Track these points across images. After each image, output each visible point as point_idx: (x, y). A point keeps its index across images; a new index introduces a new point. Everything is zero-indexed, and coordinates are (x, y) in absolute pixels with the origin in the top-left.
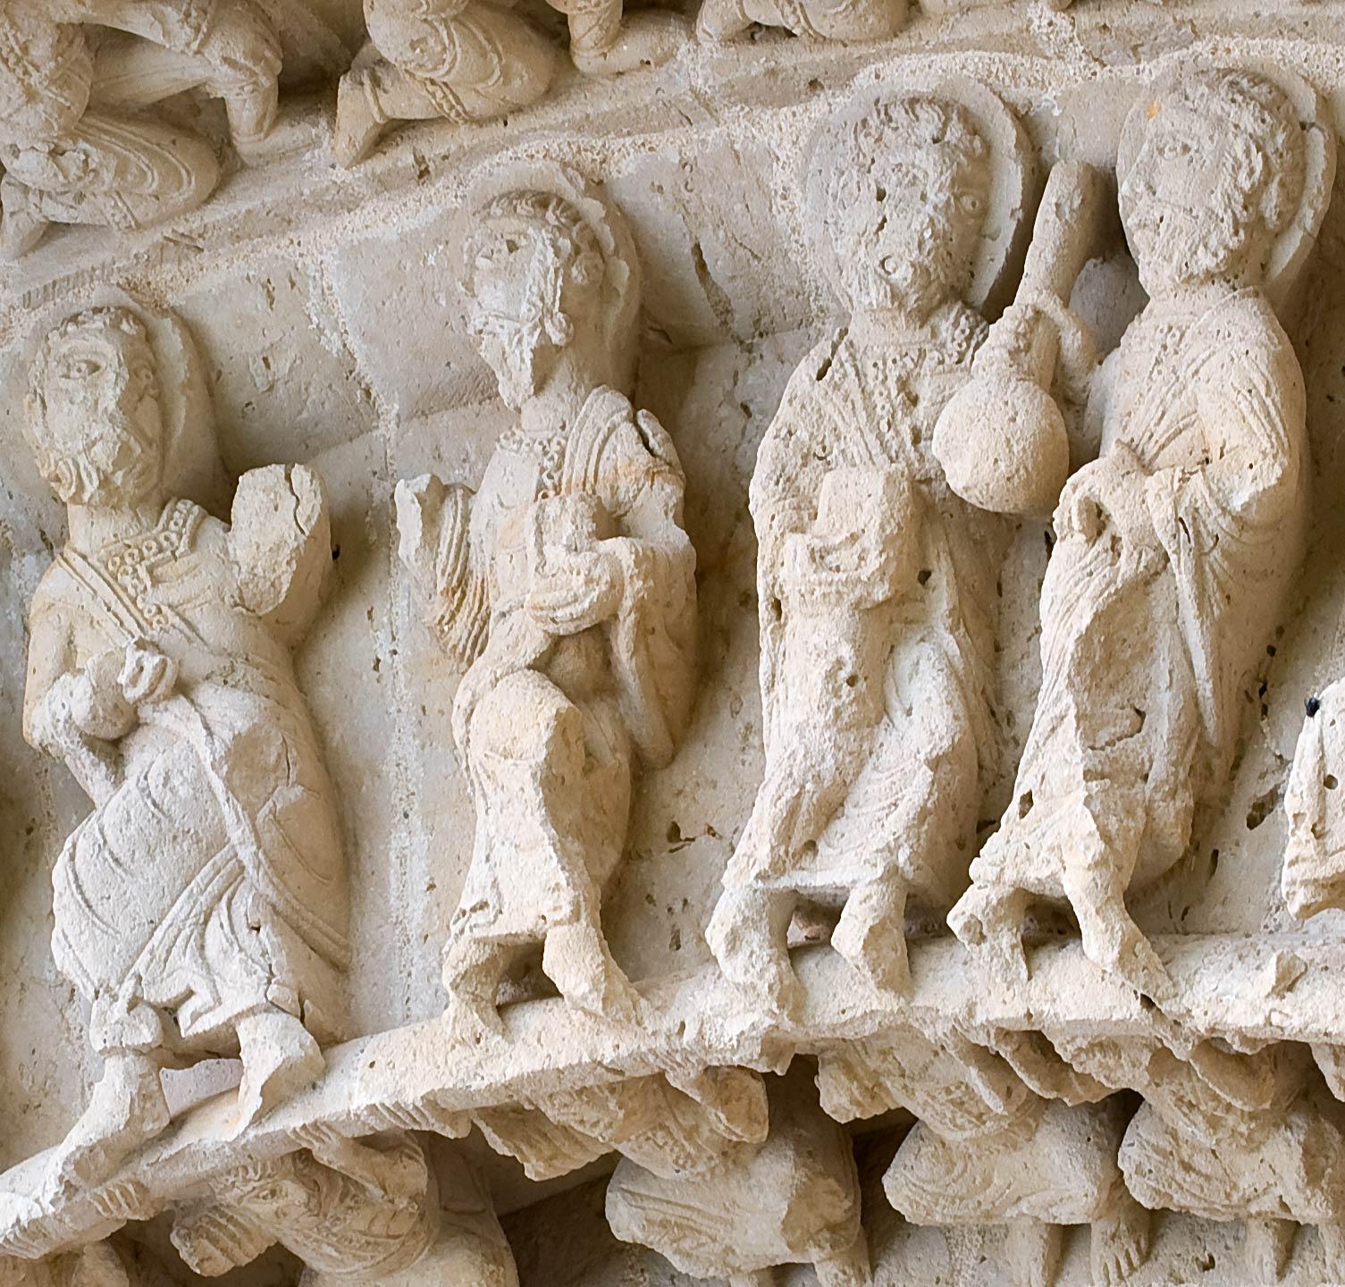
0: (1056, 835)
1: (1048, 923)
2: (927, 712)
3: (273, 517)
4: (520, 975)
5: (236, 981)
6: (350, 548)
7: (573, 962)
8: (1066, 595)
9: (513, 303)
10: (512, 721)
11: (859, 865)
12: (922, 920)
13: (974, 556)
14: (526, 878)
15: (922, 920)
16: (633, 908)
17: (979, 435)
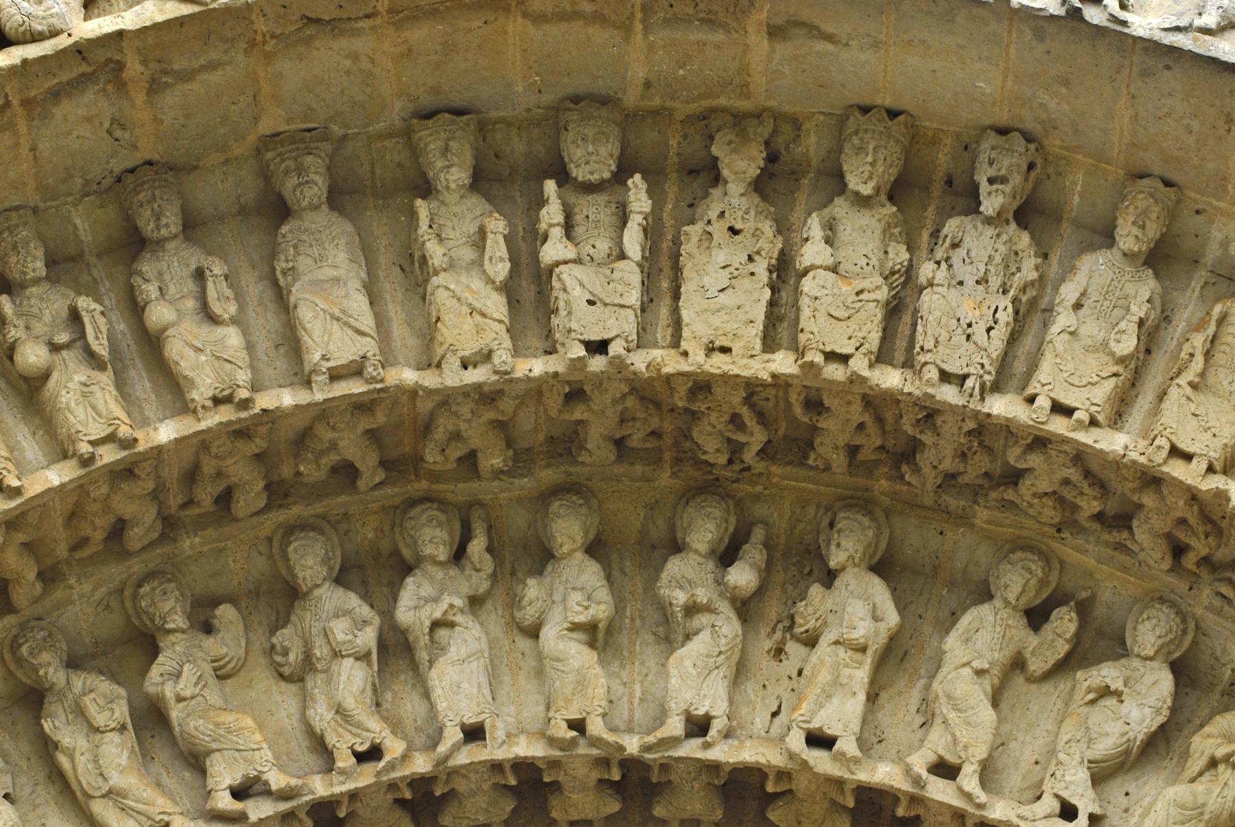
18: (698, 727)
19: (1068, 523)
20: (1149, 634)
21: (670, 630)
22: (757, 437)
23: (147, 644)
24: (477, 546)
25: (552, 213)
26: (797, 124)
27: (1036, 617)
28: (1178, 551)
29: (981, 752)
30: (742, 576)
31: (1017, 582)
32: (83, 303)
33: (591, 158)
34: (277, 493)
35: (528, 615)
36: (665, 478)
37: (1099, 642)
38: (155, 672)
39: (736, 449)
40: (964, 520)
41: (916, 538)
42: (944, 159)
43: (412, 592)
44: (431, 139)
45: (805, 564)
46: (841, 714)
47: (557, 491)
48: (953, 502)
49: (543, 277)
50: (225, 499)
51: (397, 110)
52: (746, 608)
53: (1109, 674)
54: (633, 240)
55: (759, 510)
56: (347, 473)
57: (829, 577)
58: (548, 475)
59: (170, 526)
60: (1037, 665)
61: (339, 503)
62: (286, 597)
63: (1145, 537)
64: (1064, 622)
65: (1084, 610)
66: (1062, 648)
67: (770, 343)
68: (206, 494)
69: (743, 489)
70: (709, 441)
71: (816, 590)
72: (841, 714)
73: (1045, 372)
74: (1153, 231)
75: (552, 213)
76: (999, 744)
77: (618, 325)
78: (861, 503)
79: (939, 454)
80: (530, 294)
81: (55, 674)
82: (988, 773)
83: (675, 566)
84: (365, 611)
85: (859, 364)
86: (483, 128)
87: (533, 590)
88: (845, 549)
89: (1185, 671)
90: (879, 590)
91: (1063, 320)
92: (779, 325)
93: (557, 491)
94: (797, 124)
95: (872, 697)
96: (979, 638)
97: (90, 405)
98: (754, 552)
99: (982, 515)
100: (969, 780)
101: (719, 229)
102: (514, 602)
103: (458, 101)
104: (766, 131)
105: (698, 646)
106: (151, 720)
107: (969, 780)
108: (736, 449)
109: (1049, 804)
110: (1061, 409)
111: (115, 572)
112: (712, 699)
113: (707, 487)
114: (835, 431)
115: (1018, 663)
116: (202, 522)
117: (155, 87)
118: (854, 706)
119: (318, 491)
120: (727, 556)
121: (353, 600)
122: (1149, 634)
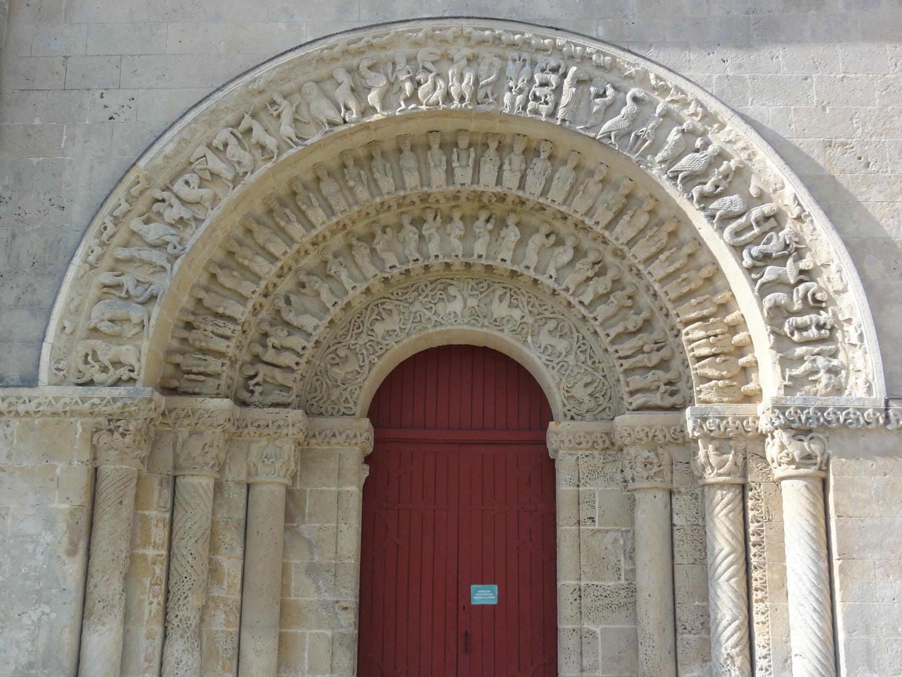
0: (627, 364)
1: (622, 365)
2: (629, 353)
3: (629, 303)
4: (608, 335)
5: (600, 319)
6: (630, 308)
7: (609, 339)
8: (639, 357)
9: (645, 315)
10: (619, 328)
11: (621, 354)
12: (620, 358)
13: (640, 351)
14: (613, 333)
15: (620, 358)
16: (613, 342)
17: (646, 348)
18: (480, 256)
19: (555, 218)
20: (570, 242)
21: (476, 237)
22: (495, 199)
23: (373, 236)
24: (438, 218)
25: (455, 157)
26: (505, 136)
27: (548, 236)
28: (576, 225)
29: (534, 265)
30: (490, 226)
31: (545, 229)
32: (361, 172)
33: (463, 142)
34: (399, 205)
35: (448, 232)
36: (476, 204)
37: (560, 242)
38: (375, 242)
39: (490, 201)
40: (535, 215)
41: (525, 218)
42: (534, 145)
43: (425, 226)
44: (431, 137)
45: (502, 223)
46: (508, 255)
47: (455, 206)
48: (533, 212)
49: (453, 169)
50: (389, 207)
51: (425, 131)
52: (490, 232)
53: (560, 249)
54: (471, 162)
55: (494, 211)
56: (413, 203)
57: (507, 226)
58: (453, 203)
59: (378, 212)
60: (548, 245)
61: (411, 208)
62: (400, 227)
63: (570, 222)
64: (553, 239)
65: (557, 235)
66: (552, 243)
67: (497, 184)
68: (385, 207)
69: (491, 207)
70: (485, 199)
71: (504, 229)
72: (508, 255)
73: (550, 194)
74: (575, 163)
75: (455, 157)
76: (539, 262)
77: (468, 180)
78: (514, 211)
79: (529, 205)
80: (450, 172)
81: (354, 242)
82: (536, 270)
83: (477, 223)
84: (416, 231)
85: (514, 191)
86: (442, 135)
87: (449, 226)
88: (512, 220)
89: (576, 249)
90: (517, 230)
91: (555, 182)
92: (499, 181)
93: (455, 206)
94: (505, 136)
95: (515, 251)
96: (537, 240)
97: (362, 193)
98: (493, 221)
99: (538, 215)
100: (532, 270)
101: (488, 159)
102: (445, 228)
103: (436, 129)
104: (498, 138)
105: (481, 240)
106: (373, 251)
107: (532, 270)
108: (490, 201)
109: (547, 275)
110: (553, 201)
111: (367, 221)
112: (483, 252)
113: (484, 207)
114: (509, 200)
115: (544, 245)
116: (385, 211)
117: (376, 130)
118: (510, 254)
119: (408, 205)
120: (488, 221)
121: (414, 229)
122: (570, 242)
